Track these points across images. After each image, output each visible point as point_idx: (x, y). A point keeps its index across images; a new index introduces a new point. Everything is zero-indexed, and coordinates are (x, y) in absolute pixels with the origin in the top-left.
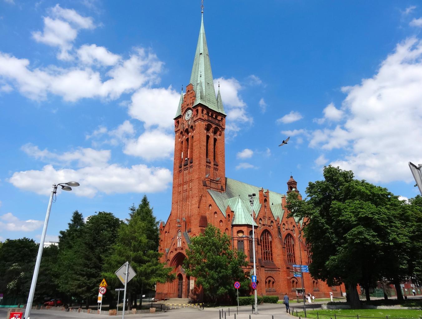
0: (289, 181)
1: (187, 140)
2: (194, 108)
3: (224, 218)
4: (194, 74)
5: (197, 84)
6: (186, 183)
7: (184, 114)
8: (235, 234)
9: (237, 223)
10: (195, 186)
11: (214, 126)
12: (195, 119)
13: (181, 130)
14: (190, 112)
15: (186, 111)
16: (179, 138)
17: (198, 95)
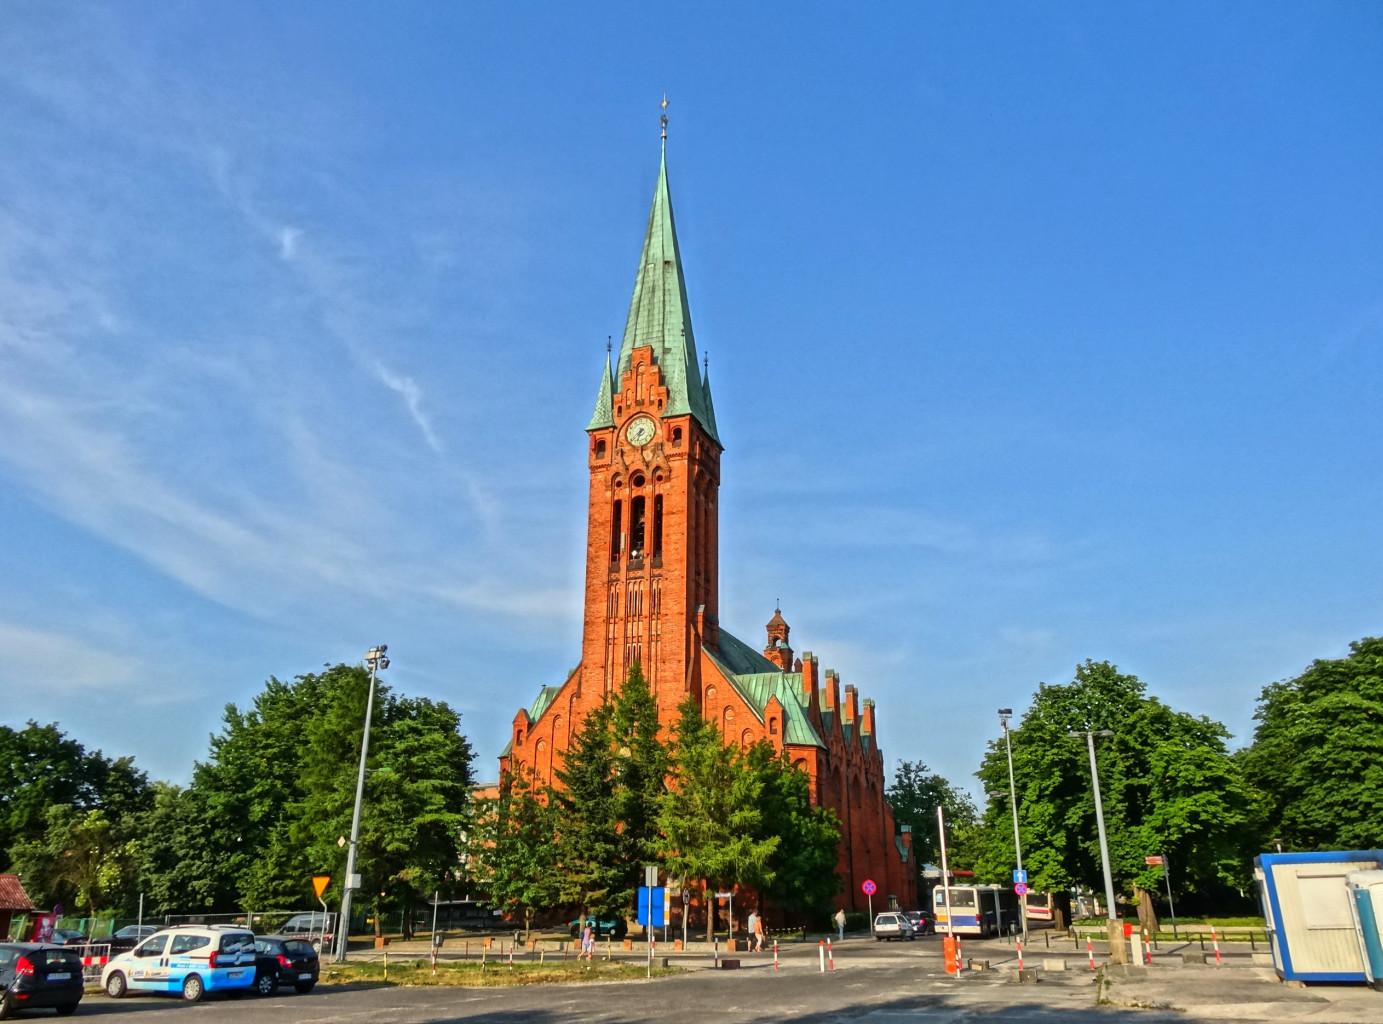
0: (772, 621)
1: (638, 504)
2: (662, 418)
3: (758, 723)
4: (646, 313)
5: (666, 351)
7: (623, 425)
9: (795, 741)
11: (708, 477)
15: (631, 419)
16: (606, 490)
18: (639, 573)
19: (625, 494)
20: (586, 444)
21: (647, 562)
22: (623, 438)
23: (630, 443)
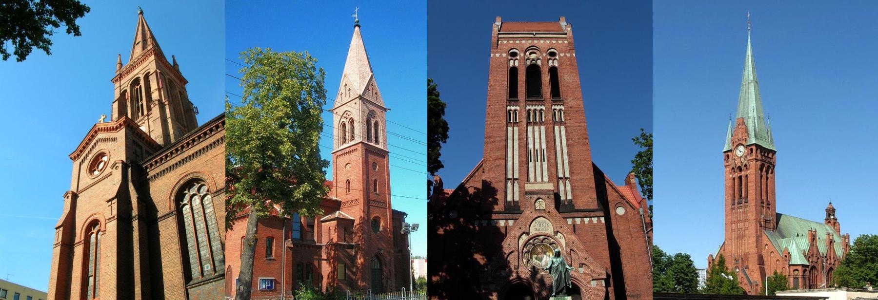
1: (740, 178)
5: (749, 118)
6: (741, 221)
8: (792, 273)
10: (751, 227)
11: (766, 165)
12: (749, 158)
13: (733, 166)
14: (742, 148)
15: (737, 146)
17: (752, 133)
19: (736, 175)
20: (723, 156)
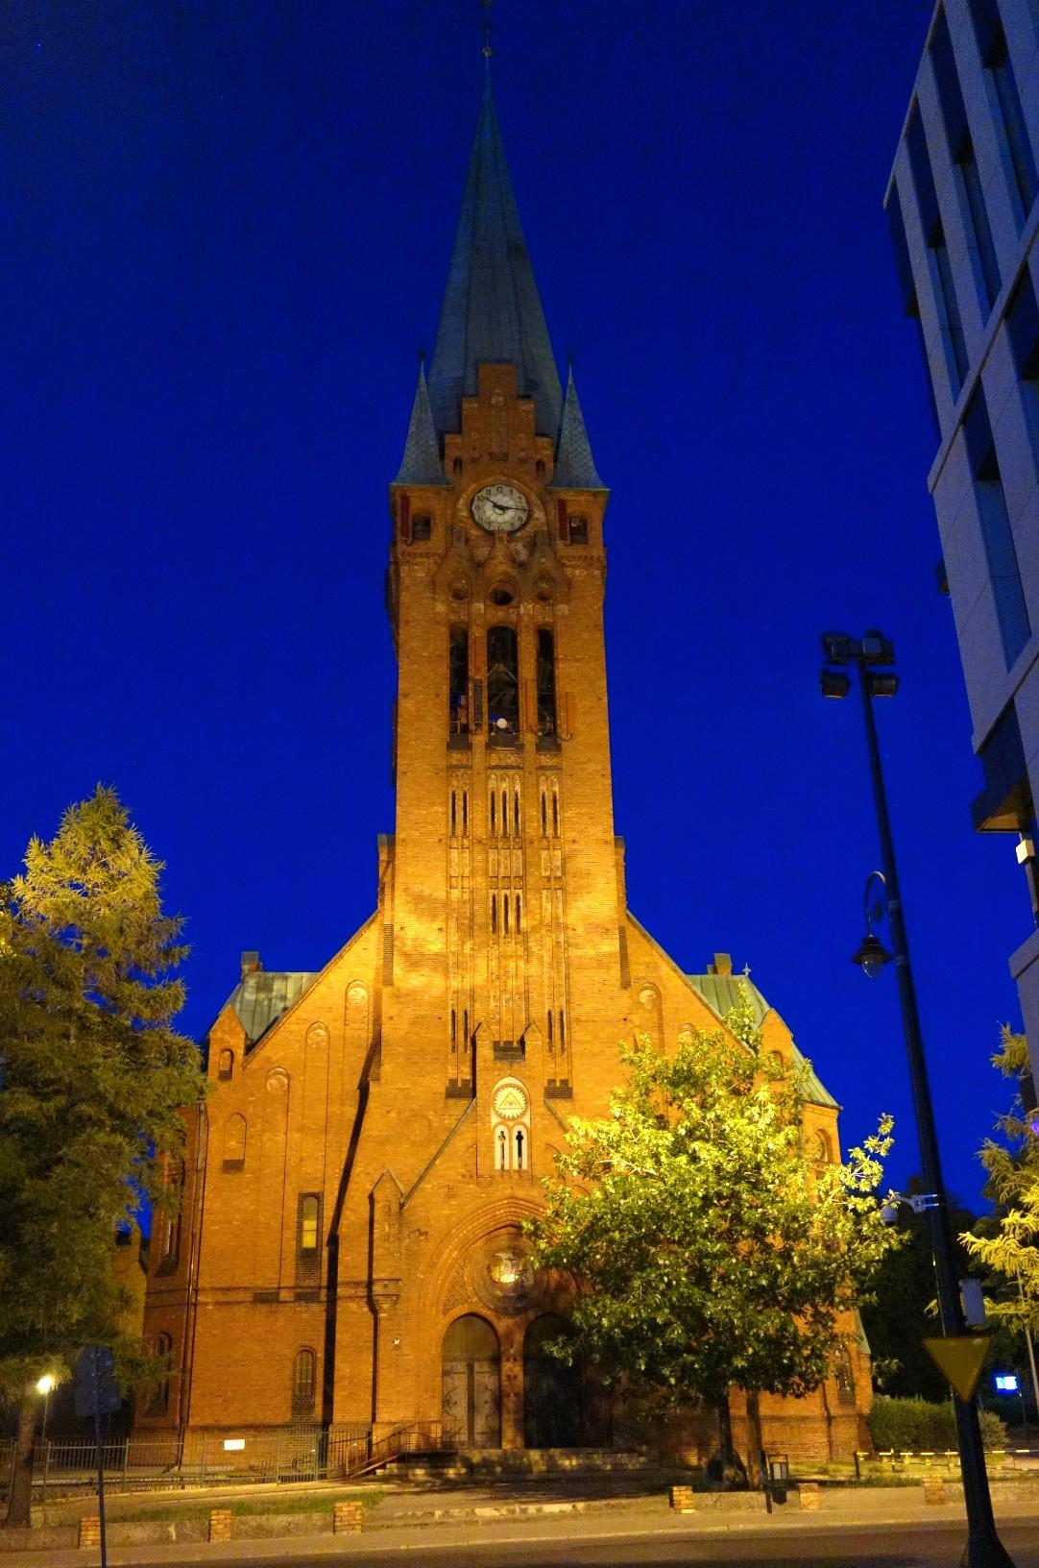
18: (512, 759)
21: (529, 739)
22: (465, 513)
23: (482, 528)
